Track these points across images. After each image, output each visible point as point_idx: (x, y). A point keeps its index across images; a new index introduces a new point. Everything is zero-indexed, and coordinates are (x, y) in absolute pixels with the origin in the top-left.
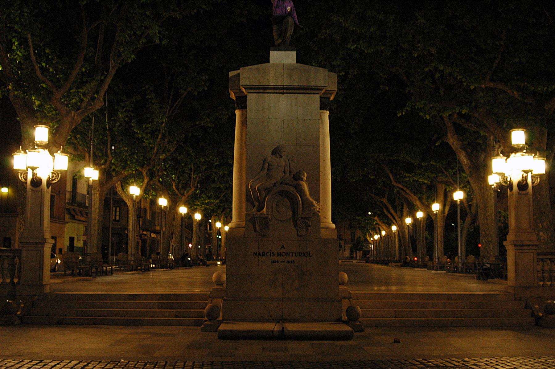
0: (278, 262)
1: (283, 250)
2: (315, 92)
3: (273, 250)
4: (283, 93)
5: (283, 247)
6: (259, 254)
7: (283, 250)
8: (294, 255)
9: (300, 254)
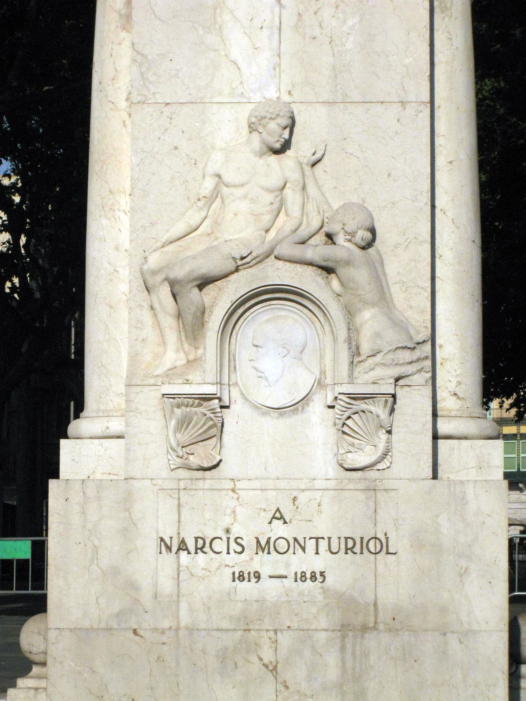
0: (258, 576)
3: (236, 531)
6: (183, 546)
8: (323, 545)
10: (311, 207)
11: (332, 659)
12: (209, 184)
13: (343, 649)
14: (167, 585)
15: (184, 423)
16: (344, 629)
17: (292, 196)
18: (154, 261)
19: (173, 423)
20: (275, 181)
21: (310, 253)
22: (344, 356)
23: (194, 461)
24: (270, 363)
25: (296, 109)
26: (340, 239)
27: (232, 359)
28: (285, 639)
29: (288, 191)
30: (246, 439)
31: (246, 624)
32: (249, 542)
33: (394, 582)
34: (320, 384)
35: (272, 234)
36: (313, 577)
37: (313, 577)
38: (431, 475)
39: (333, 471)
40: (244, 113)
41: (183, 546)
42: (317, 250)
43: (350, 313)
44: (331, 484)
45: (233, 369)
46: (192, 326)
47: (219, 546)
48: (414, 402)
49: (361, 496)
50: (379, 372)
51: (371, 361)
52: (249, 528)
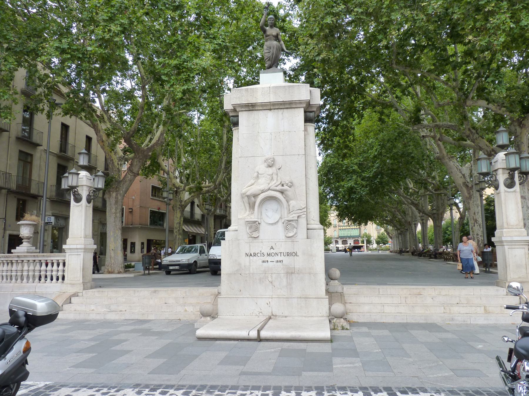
0: (268, 261)
1: (272, 251)
2: (298, 106)
4: (270, 109)
5: (272, 248)
6: (251, 255)
7: (272, 251)
8: (282, 254)
9: (288, 254)
10: (279, 178)
11: (285, 280)
12: (256, 174)
13: (287, 278)
14: (248, 264)
15: (250, 228)
16: (287, 273)
17: (275, 177)
18: (244, 191)
19: (248, 228)
20: (270, 173)
21: (278, 188)
22: (286, 211)
23: (253, 236)
24: (270, 213)
25: (275, 157)
26: (285, 185)
27: (261, 213)
28: (274, 276)
29: (274, 175)
30: (265, 232)
31: (265, 272)
32: (266, 254)
33: (298, 262)
34: (281, 218)
35: (270, 185)
36: (280, 261)
37: (280, 261)
38: (306, 237)
39: (284, 237)
40: (264, 158)
41: (251, 255)
42: (280, 188)
43: (288, 202)
44: (284, 240)
45: (261, 215)
46: (252, 206)
47: (259, 255)
48: (303, 221)
49: (290, 243)
50: (294, 215)
51: (292, 213)
52: (266, 250)
